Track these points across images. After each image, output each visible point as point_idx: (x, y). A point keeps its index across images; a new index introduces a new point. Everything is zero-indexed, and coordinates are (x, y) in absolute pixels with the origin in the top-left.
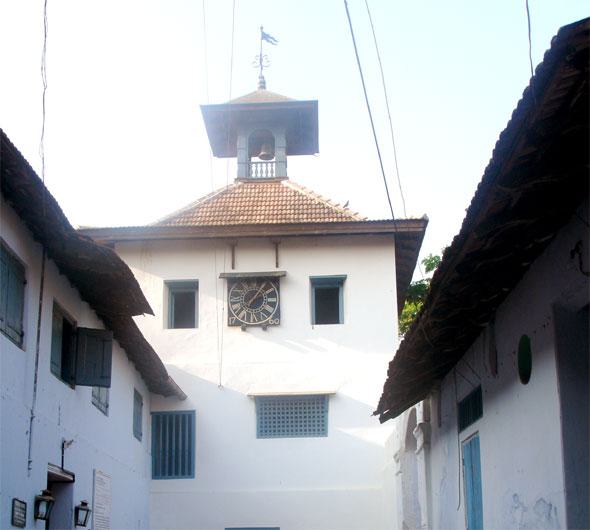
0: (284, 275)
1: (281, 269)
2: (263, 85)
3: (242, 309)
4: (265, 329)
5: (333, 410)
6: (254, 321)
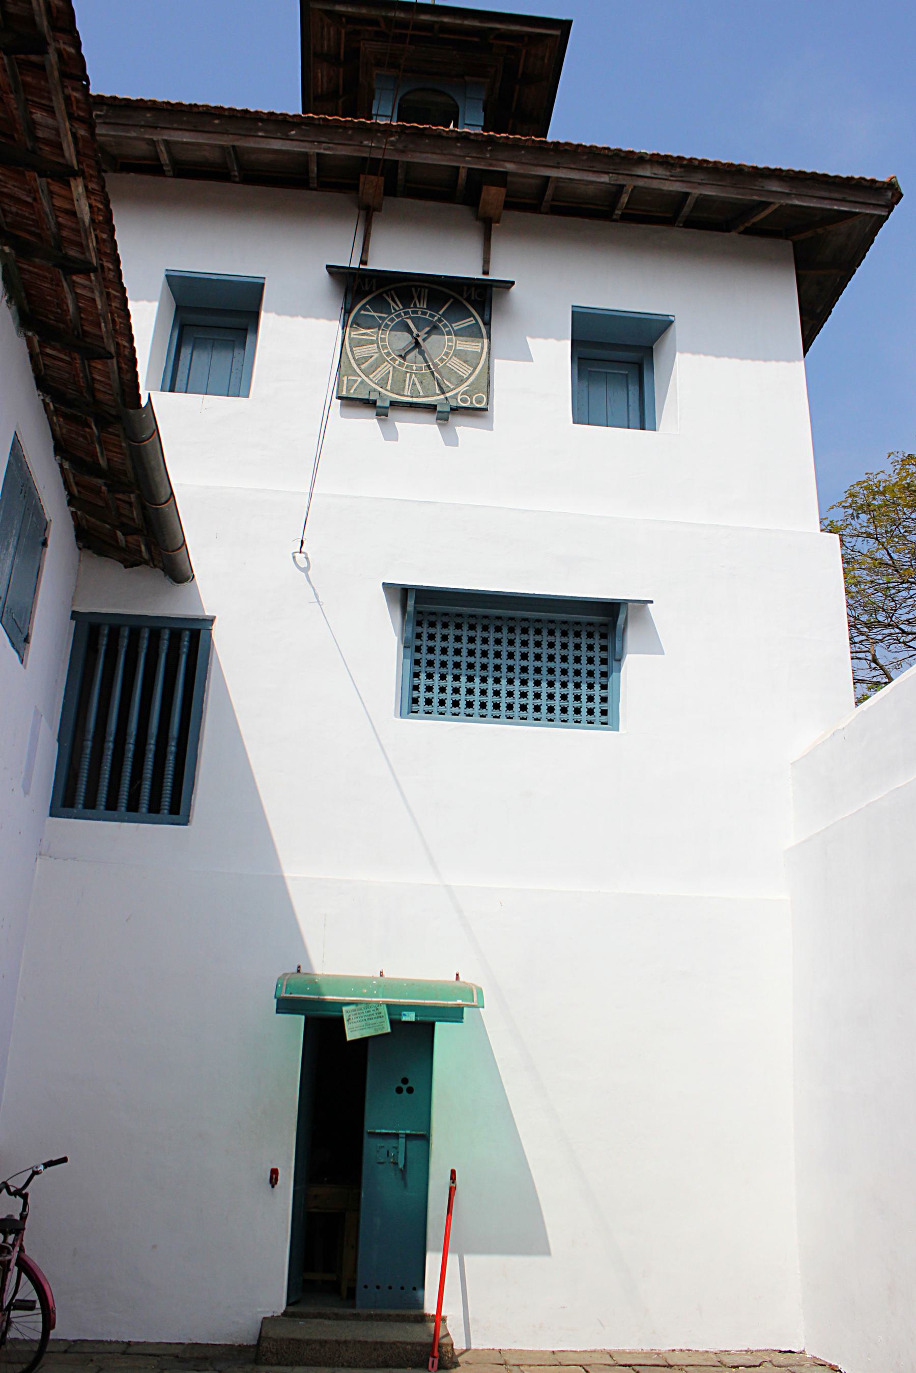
1: (495, 275)
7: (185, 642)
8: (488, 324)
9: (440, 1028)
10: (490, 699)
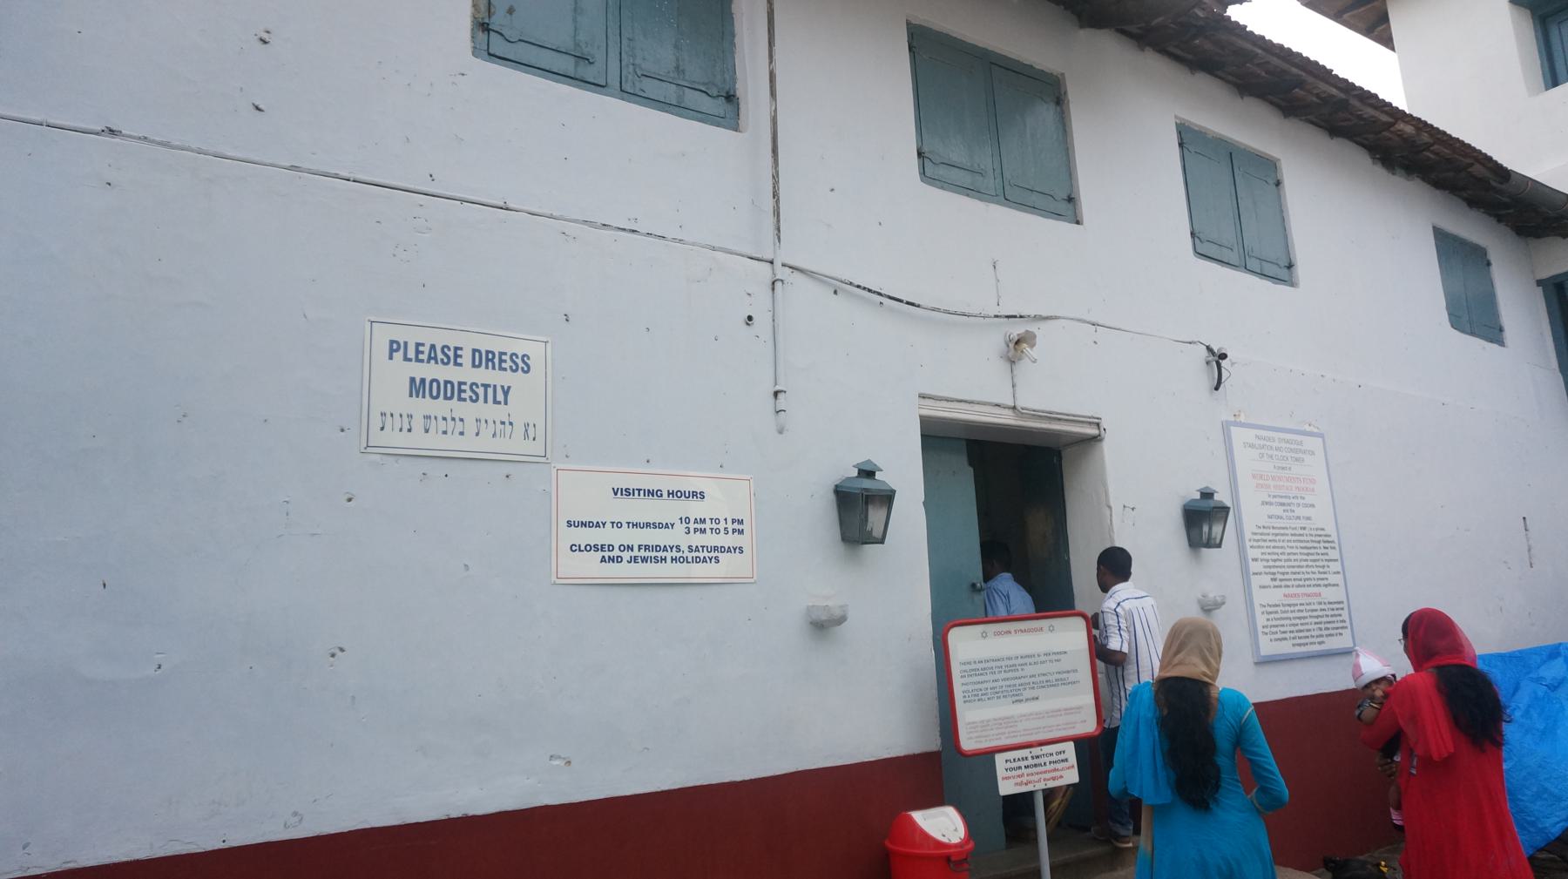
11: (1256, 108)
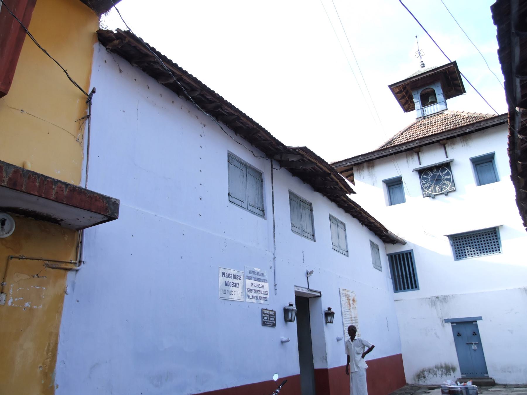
0: (452, 161)
2: (423, 66)
3: (430, 187)
4: (447, 195)
5: (503, 235)
6: (439, 192)
7: (409, 255)
8: (451, 170)
9: (479, 322)
10: (473, 253)
11: (341, 211)
